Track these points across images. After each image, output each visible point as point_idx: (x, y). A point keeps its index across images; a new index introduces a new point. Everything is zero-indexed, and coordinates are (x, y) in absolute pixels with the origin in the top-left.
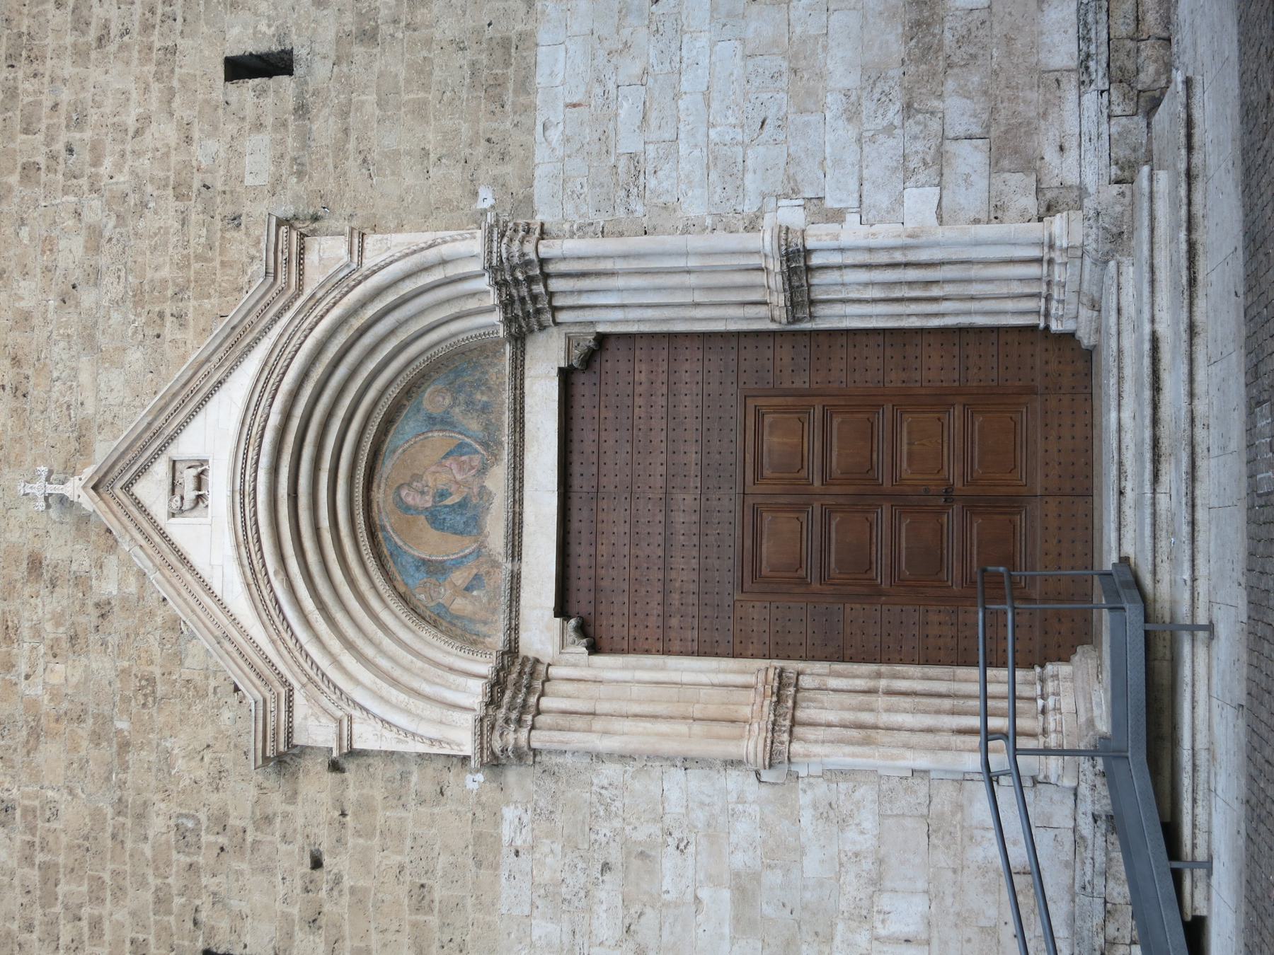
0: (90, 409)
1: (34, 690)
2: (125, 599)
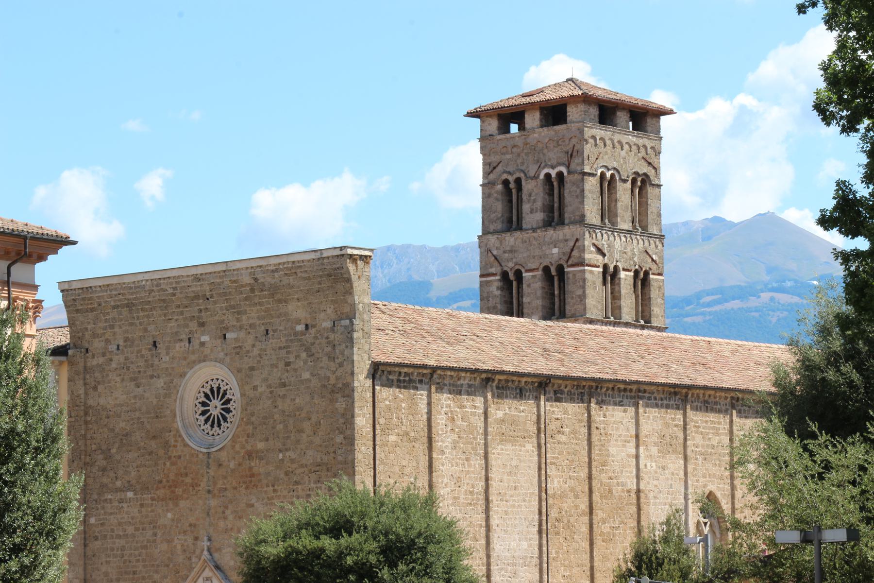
0: (223, 551)
1: (176, 541)
2: (191, 564)
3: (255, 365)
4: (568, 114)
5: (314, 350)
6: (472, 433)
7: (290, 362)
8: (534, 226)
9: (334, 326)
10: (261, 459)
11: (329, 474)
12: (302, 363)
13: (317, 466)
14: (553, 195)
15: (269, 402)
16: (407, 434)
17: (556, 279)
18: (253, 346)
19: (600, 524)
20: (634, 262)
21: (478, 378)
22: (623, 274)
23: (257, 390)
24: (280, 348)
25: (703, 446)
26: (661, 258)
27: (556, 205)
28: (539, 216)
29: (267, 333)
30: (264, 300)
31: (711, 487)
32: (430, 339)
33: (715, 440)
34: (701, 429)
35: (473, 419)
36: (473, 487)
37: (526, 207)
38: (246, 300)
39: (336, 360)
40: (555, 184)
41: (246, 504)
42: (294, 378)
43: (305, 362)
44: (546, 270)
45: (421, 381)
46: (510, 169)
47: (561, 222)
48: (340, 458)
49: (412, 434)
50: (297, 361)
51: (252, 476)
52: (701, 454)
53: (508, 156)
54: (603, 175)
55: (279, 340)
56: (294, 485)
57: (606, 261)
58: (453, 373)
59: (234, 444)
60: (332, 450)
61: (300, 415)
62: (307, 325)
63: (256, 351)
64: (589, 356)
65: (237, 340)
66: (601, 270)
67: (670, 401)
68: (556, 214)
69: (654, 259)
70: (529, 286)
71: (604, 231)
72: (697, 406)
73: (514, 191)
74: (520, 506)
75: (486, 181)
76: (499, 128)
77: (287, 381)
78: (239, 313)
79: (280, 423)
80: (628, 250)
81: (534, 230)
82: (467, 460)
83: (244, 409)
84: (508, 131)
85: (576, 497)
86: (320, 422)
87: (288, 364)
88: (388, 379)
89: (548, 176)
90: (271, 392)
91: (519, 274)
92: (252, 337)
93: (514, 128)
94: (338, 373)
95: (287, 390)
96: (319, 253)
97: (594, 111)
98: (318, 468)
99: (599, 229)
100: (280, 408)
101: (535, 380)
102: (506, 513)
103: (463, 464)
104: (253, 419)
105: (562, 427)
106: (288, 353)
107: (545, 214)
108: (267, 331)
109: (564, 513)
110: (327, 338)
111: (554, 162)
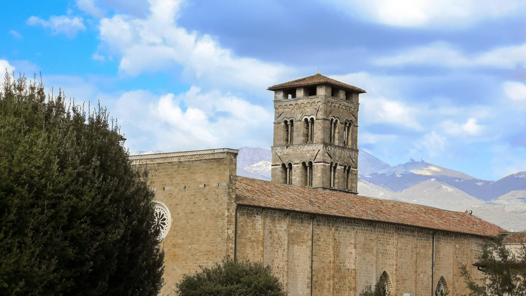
3: (178, 203)
4: (317, 91)
5: (208, 197)
6: (279, 239)
7: (196, 202)
8: (299, 143)
9: (218, 186)
10: (180, 248)
11: (213, 256)
12: (202, 203)
13: (208, 252)
14: (308, 129)
15: (185, 221)
17: (308, 168)
18: (178, 193)
19: (335, 285)
20: (345, 162)
21: (283, 213)
22: (338, 167)
23: (179, 215)
24: (191, 195)
25: (382, 250)
26: (357, 161)
27: (310, 133)
28: (302, 138)
29: (185, 188)
30: (184, 172)
32: (259, 194)
34: (381, 242)
35: (281, 233)
36: (279, 264)
37: (295, 134)
38: (175, 172)
39: (219, 202)
40: (310, 124)
41: (172, 269)
42: (198, 209)
43: (203, 202)
44: (304, 163)
45: (257, 214)
46: (288, 116)
47: (312, 143)
48: (219, 249)
49: (252, 239)
50: (199, 202)
51: (175, 255)
53: (287, 110)
54: (332, 120)
55: (191, 191)
56: (195, 261)
57: (332, 161)
58: (272, 211)
59: (167, 240)
60: (215, 244)
61: (200, 227)
62: (205, 185)
63: (179, 196)
64: (331, 205)
65: (170, 190)
66: (330, 165)
67: (368, 228)
68: (310, 138)
69: (354, 161)
70: (295, 171)
71: (332, 147)
72: (380, 231)
73: (290, 126)
75: (276, 121)
76: (284, 96)
77: (194, 211)
78: (171, 178)
79: (190, 231)
80: (342, 156)
81: (299, 145)
83: (173, 224)
84: (287, 98)
86: (210, 231)
87: (195, 203)
89: (306, 120)
90: (186, 216)
91: (290, 165)
92: (177, 189)
93: (290, 96)
94: (220, 208)
95: (194, 216)
96: (212, 151)
97: (330, 90)
98: (208, 253)
99: (330, 146)
100: (190, 224)
104: (177, 228)
105: (319, 238)
106: (195, 197)
107: (304, 138)
108: (185, 187)
109: (319, 278)
110: (215, 191)
111: (310, 114)
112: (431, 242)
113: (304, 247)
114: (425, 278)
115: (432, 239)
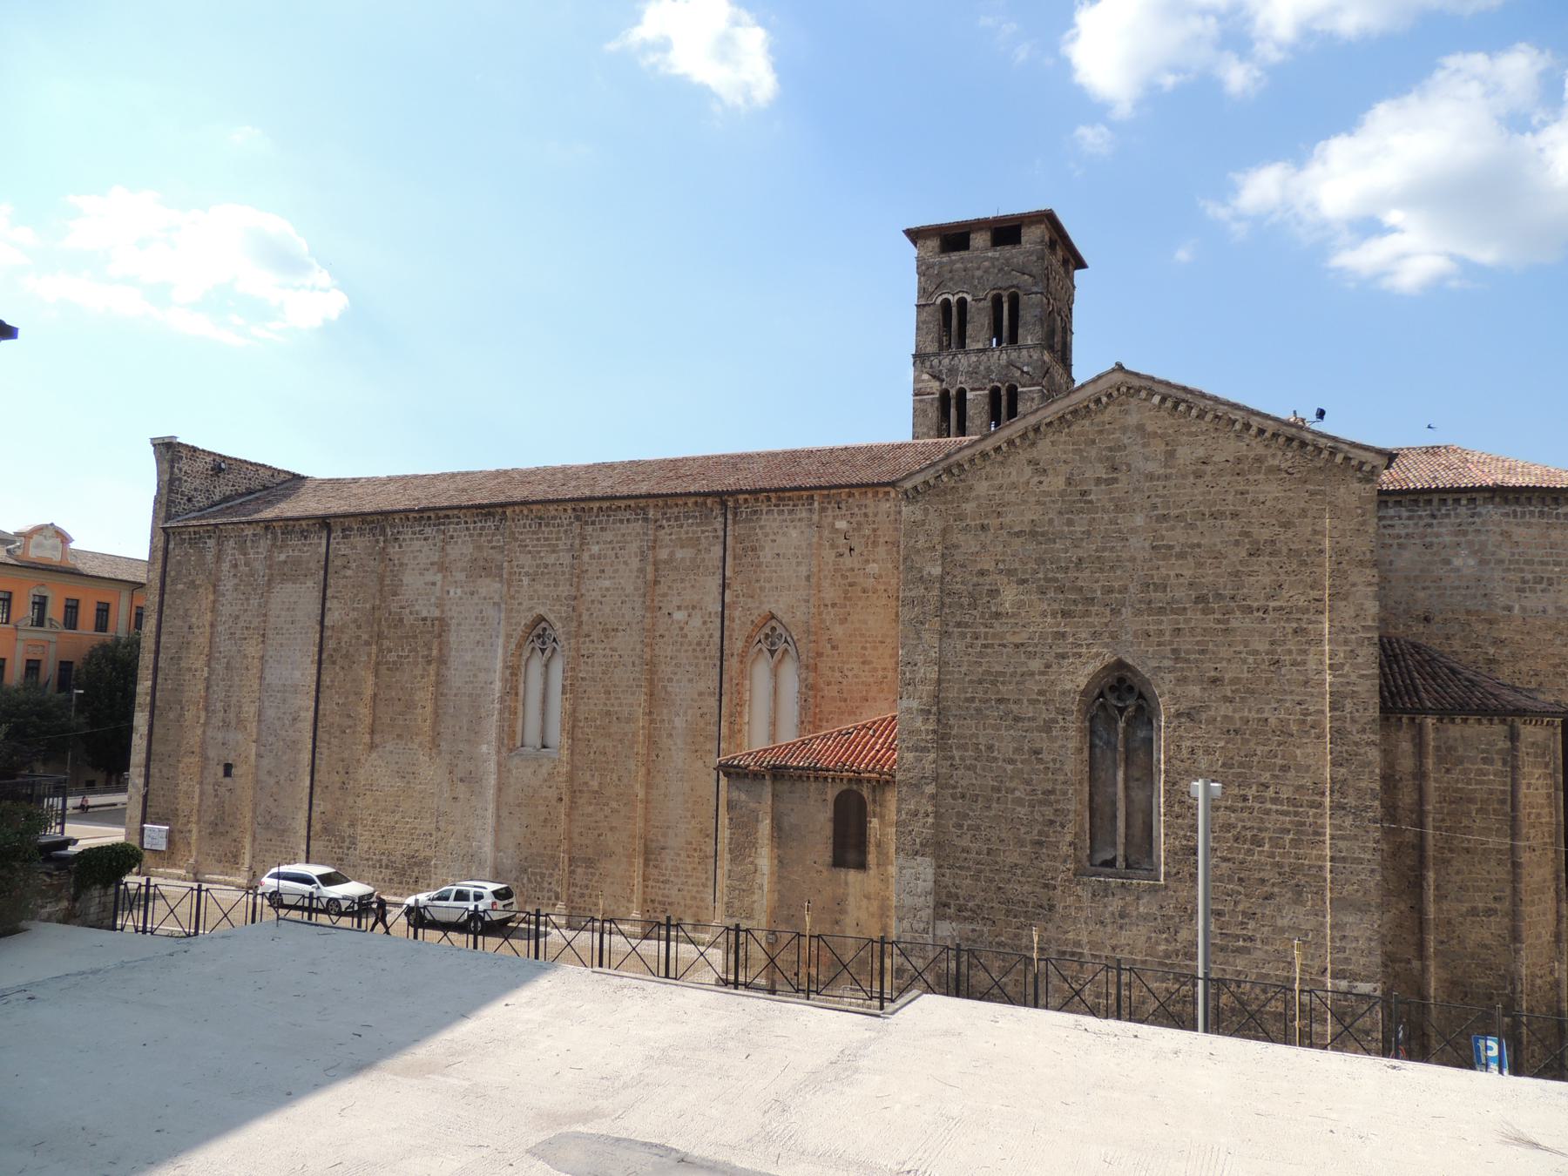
6: (253, 576)
16: (193, 582)
31: (541, 610)
33: (551, 559)
34: (530, 548)
49: (197, 582)
52: (527, 574)
72: (525, 524)
74: (295, 639)
82: (248, 599)
85: (359, 627)
88: (181, 539)
101: (313, 521)
102: (281, 645)
103: (242, 604)
109: (343, 644)
112: (720, 527)
113: (310, 584)
114: (697, 622)
115: (720, 519)
